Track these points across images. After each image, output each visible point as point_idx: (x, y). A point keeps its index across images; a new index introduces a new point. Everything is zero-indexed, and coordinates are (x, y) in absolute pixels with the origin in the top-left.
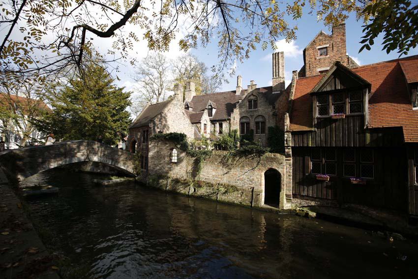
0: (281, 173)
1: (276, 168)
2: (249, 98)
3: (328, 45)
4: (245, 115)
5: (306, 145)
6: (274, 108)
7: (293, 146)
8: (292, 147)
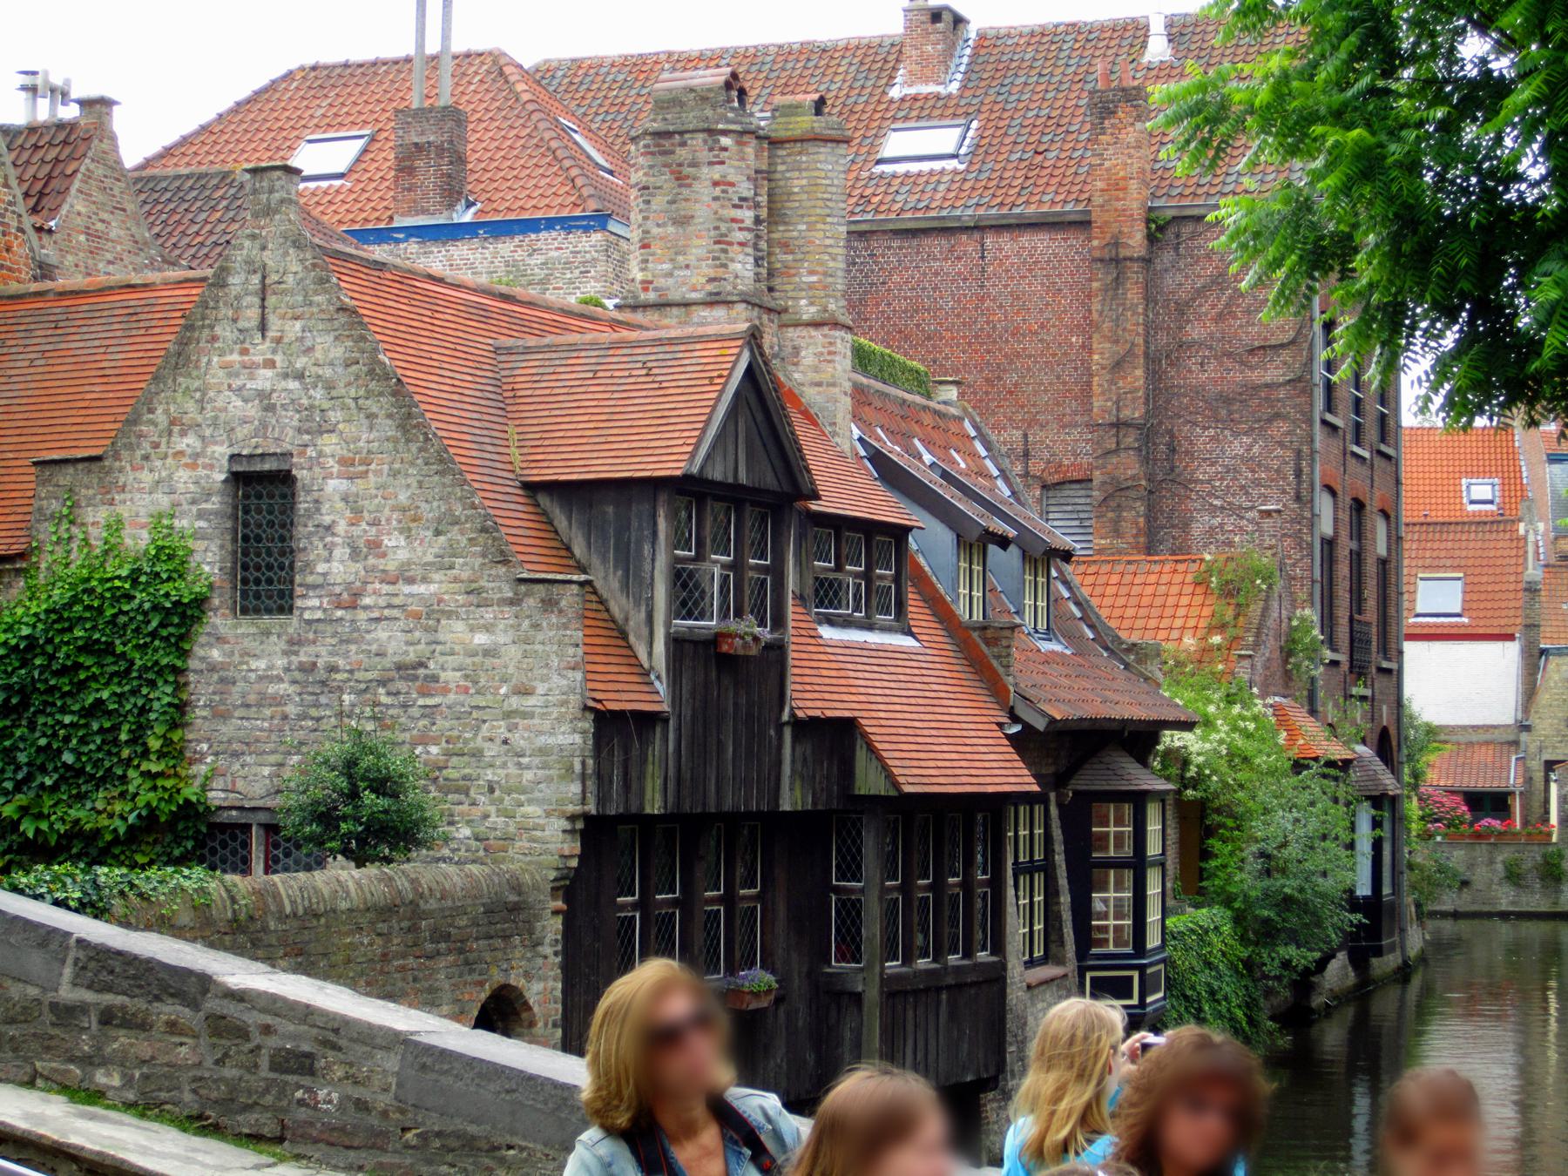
0: (536, 1009)
1: (521, 983)
5: (634, 810)
7: (594, 812)
8: (586, 817)
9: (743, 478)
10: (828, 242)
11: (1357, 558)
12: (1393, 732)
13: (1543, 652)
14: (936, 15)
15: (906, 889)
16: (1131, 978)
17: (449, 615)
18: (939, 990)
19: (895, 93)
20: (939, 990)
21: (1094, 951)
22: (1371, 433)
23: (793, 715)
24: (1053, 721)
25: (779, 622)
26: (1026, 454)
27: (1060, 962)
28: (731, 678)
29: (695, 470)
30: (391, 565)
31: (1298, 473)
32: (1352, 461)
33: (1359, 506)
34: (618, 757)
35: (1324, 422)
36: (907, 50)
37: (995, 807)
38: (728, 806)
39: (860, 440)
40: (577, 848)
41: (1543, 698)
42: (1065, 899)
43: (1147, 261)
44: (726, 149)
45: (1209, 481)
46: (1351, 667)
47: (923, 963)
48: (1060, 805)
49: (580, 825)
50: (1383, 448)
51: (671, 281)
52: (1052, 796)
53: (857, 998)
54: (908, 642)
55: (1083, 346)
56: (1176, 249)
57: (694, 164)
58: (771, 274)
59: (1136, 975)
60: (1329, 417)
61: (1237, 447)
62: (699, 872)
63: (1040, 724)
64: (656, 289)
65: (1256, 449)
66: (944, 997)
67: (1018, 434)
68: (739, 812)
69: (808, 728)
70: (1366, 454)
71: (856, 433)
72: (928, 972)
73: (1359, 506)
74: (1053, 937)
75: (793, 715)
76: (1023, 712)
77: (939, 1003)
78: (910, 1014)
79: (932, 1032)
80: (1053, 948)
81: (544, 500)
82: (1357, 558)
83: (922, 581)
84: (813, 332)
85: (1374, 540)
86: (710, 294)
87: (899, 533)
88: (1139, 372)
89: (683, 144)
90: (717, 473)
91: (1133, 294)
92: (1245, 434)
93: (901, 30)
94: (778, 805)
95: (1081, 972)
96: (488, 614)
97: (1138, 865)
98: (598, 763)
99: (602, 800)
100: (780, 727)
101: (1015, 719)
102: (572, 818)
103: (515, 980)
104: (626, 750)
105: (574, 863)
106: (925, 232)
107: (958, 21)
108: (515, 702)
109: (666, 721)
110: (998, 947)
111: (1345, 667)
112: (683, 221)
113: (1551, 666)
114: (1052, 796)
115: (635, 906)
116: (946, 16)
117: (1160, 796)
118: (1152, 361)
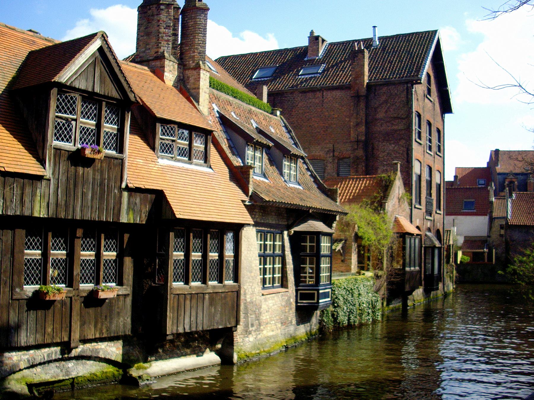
5: (27, 213)
9: (97, 90)
10: (199, 42)
11: (429, 183)
12: (441, 231)
13: (495, 218)
14: (317, 38)
16: (314, 293)
19: (306, 59)
21: (301, 284)
22: (435, 149)
23: (127, 186)
25: (120, 149)
26: (334, 151)
31: (408, 154)
32: (426, 155)
33: (430, 169)
34: (17, 191)
35: (416, 141)
36: (309, 48)
38: (88, 216)
39: (218, 111)
41: (494, 229)
42: (290, 267)
43: (367, 97)
44: (162, 10)
45: (383, 157)
46: (426, 211)
47: (193, 284)
48: (289, 235)
50: (438, 153)
51: (144, 54)
52: (286, 233)
54: (210, 170)
55: (349, 121)
56: (375, 94)
57: (153, 15)
58: (182, 53)
59: (316, 292)
60: (418, 140)
61: (391, 147)
64: (140, 57)
65: (396, 148)
66: (207, 296)
67: (332, 145)
68: (94, 221)
70: (432, 154)
71: (216, 109)
72: (197, 288)
73: (430, 169)
74: (284, 279)
75: (127, 186)
77: (204, 298)
78: (188, 302)
79: (200, 308)
80: (284, 283)
82: (429, 183)
84: (195, 72)
85: (435, 178)
86: (155, 57)
88: (364, 127)
89: (150, 9)
90: (82, 85)
91: (362, 105)
92: (393, 143)
93: (307, 44)
94: (119, 219)
95: (297, 291)
97: (317, 256)
104: (23, 189)
106: (308, 92)
107: (323, 41)
109: (49, 180)
110: (236, 279)
111: (424, 210)
112: (148, 34)
113: (496, 221)
114: (286, 233)
116: (320, 39)
117: (329, 235)
118: (367, 123)
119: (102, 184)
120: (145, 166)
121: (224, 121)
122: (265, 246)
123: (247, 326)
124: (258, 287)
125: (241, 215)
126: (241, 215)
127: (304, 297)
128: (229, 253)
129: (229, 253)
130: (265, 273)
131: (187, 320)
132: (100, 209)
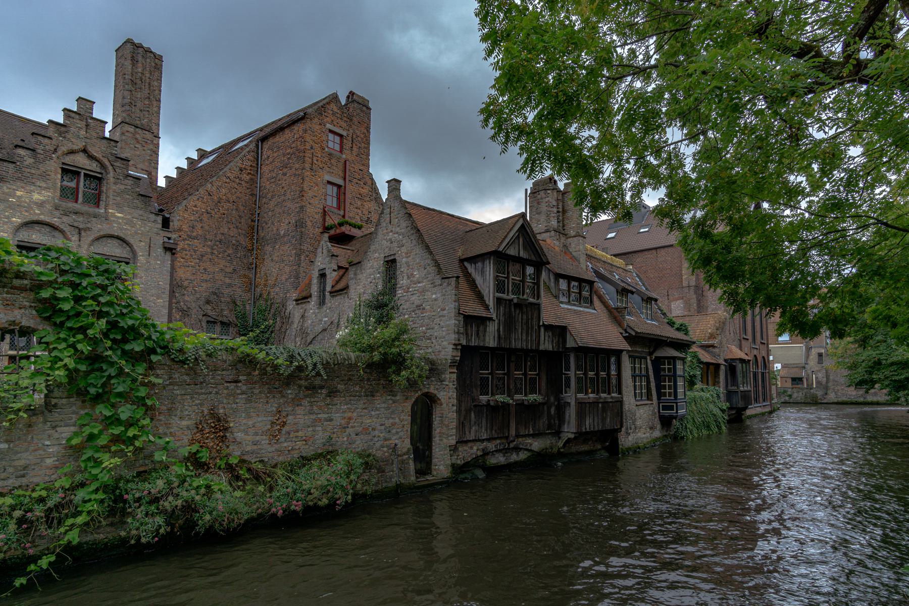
1: (436, 392)
2: (69, 159)
3: (344, 133)
4: (42, 218)
6: (166, 223)
7: (464, 343)
8: (463, 346)
15: (585, 374)
17: (427, 291)
18: (598, 403)
20: (598, 403)
24: (636, 332)
25: (539, 297)
27: (652, 400)
28: (519, 312)
29: (500, 249)
30: (415, 279)
37: (618, 353)
38: (519, 347)
40: (459, 354)
41: (811, 357)
42: (653, 385)
47: (591, 395)
49: (459, 347)
53: (569, 404)
62: (512, 365)
63: (634, 334)
69: (548, 328)
76: (629, 330)
81: (466, 264)
83: (600, 298)
87: (591, 283)
90: (512, 252)
95: (659, 403)
96: (435, 289)
97: (674, 377)
98: (466, 330)
99: (468, 340)
100: (539, 327)
101: (626, 332)
102: (454, 345)
103: (432, 390)
105: (458, 358)
108: (441, 313)
110: (620, 392)
111: (750, 340)
115: (489, 374)
119: (527, 323)
120: (556, 309)
121: (596, 272)
122: (635, 368)
123: (627, 429)
124: (633, 400)
125: (620, 344)
126: (620, 344)
127: (665, 408)
128: (613, 373)
129: (613, 373)
130: (635, 390)
131: (587, 423)
132: (527, 340)
